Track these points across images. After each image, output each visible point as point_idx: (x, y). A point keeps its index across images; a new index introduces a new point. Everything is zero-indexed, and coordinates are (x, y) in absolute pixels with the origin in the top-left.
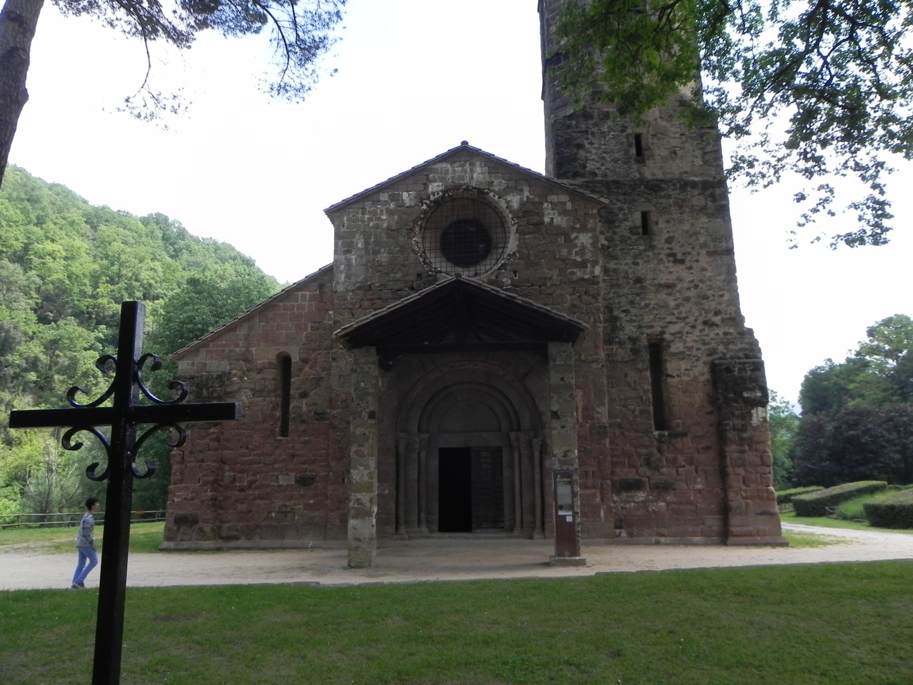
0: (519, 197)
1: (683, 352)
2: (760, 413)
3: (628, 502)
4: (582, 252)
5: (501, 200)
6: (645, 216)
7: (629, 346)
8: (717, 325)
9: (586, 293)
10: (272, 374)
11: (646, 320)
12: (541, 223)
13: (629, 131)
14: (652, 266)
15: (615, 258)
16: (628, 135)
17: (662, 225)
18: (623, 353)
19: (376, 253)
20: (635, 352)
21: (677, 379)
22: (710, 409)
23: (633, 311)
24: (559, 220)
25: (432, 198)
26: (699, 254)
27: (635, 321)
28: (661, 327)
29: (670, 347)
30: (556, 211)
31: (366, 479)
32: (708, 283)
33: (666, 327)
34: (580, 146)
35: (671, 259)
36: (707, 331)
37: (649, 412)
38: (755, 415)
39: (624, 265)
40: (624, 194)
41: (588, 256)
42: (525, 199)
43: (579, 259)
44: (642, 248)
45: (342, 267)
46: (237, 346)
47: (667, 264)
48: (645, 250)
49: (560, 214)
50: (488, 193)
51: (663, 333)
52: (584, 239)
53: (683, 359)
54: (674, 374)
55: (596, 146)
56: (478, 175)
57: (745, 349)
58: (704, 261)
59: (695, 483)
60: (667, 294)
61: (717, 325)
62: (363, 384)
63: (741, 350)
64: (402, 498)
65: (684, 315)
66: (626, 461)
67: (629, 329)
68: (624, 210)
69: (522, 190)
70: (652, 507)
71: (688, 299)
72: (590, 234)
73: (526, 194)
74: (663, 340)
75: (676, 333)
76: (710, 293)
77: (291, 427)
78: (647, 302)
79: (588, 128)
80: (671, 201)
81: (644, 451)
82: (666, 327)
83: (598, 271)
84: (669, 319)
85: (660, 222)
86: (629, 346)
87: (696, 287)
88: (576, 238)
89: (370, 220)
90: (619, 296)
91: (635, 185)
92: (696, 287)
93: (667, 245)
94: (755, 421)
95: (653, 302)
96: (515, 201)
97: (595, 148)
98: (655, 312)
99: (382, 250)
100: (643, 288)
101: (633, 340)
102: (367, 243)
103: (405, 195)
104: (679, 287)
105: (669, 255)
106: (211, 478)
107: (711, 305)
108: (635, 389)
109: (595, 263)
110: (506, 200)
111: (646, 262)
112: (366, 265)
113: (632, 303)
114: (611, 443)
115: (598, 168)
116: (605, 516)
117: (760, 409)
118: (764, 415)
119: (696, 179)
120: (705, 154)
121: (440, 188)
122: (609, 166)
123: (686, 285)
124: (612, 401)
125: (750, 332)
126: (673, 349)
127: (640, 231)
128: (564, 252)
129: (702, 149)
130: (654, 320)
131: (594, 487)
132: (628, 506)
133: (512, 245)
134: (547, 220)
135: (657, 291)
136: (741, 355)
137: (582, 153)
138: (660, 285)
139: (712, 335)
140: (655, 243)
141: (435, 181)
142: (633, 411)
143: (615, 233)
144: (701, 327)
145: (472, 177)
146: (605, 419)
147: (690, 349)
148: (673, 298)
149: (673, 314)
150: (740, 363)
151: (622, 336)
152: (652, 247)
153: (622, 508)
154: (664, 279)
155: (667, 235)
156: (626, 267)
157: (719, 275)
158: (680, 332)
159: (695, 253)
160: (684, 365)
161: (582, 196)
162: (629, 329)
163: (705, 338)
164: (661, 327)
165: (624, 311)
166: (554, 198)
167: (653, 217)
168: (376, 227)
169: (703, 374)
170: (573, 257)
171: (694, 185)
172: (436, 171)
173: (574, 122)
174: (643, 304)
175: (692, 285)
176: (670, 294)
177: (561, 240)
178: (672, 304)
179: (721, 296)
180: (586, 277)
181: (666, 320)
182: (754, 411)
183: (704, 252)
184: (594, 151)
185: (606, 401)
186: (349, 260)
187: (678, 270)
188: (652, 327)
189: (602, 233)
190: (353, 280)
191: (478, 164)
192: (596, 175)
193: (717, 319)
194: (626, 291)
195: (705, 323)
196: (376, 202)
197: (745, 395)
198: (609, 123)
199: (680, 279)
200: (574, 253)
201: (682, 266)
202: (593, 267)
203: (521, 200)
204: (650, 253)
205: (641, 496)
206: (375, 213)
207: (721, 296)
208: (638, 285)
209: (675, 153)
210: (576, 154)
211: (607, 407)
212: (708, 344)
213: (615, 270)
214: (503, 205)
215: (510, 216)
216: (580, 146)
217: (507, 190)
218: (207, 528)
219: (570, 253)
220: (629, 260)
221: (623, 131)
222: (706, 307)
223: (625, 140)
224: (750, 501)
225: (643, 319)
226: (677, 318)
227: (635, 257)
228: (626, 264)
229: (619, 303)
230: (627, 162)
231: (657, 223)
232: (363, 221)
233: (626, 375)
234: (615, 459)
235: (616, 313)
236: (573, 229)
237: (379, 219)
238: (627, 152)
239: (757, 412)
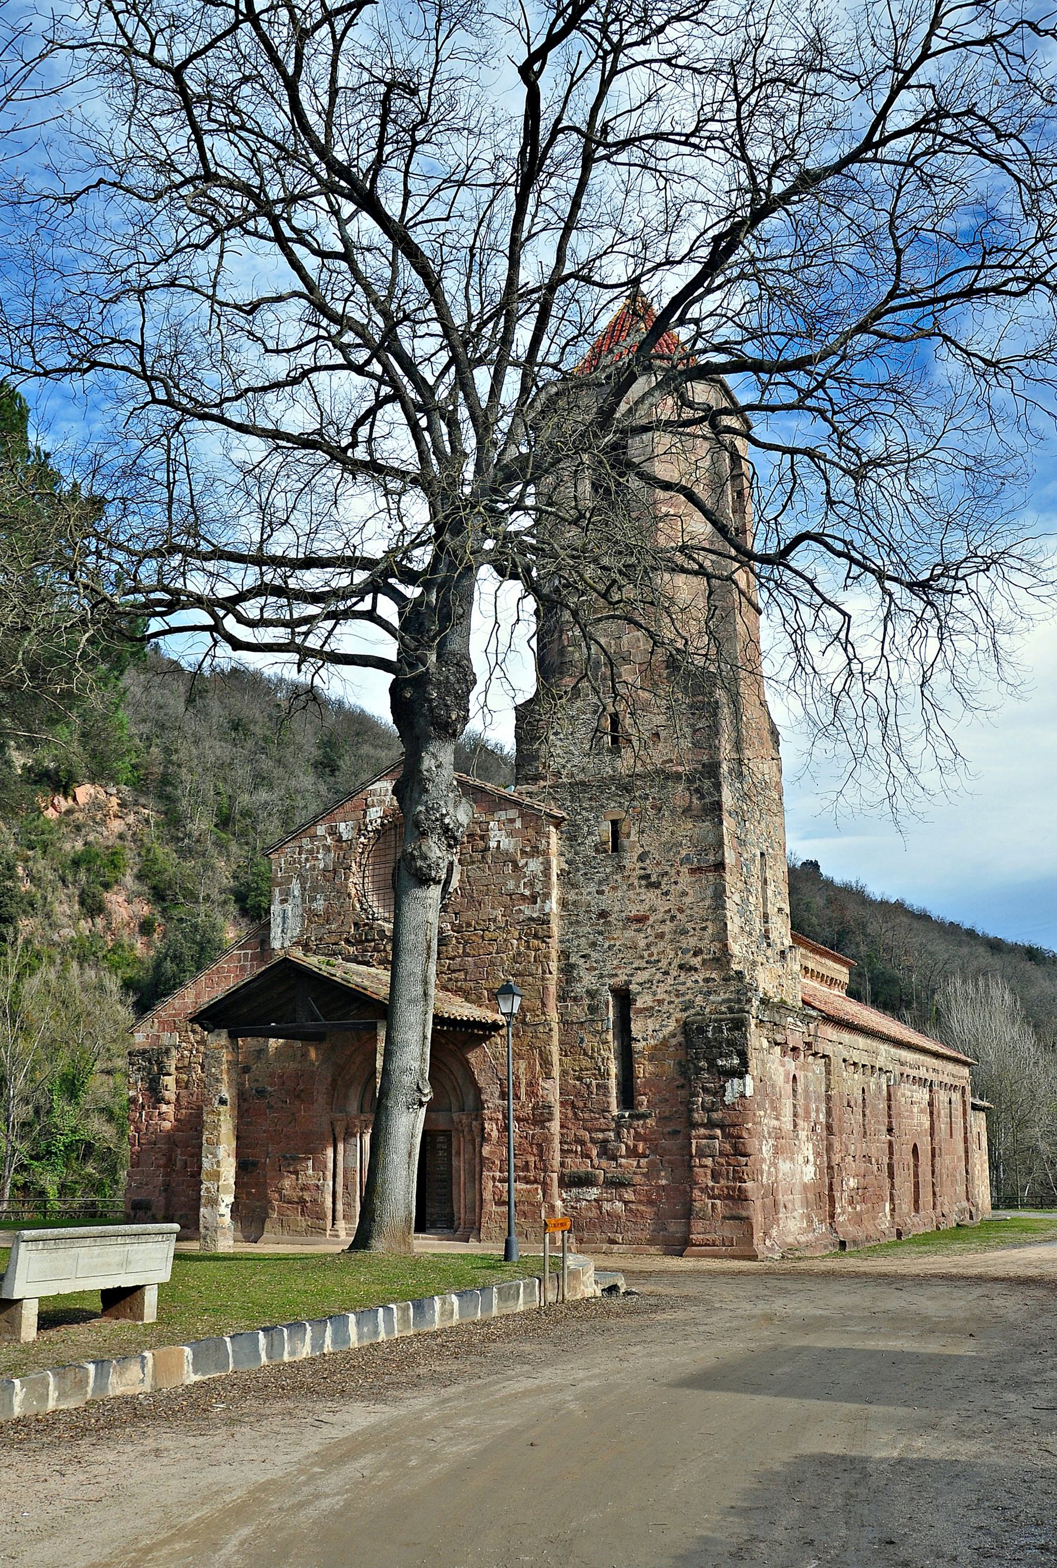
1: (652, 1008)
4: (531, 884)
6: (615, 823)
7: (587, 1001)
8: (696, 970)
9: (536, 936)
11: (609, 967)
12: (487, 849)
14: (620, 894)
15: (574, 886)
17: (634, 838)
18: (579, 1012)
19: (313, 899)
20: (593, 1009)
22: (681, 1081)
23: (595, 955)
24: (507, 844)
26: (678, 873)
32: (689, 912)
33: (632, 975)
35: (643, 882)
36: (682, 979)
37: (606, 1087)
38: (729, 1089)
39: (587, 893)
40: (590, 799)
43: (527, 893)
47: (638, 890)
51: (628, 983)
52: (534, 865)
57: (729, 1000)
58: (685, 879)
59: (659, 1178)
61: (696, 970)
63: (724, 1001)
65: (655, 957)
70: (607, 1206)
71: (661, 936)
74: (628, 991)
76: (689, 926)
81: (600, 1136)
82: (632, 975)
83: (553, 906)
85: (633, 832)
86: (587, 1001)
87: (673, 918)
89: (307, 860)
91: (603, 784)
92: (673, 918)
98: (621, 955)
100: (607, 923)
101: (592, 994)
102: (303, 889)
103: (343, 825)
104: (650, 922)
105: (641, 878)
106: (161, 1162)
107: (692, 942)
108: (592, 1058)
109: (547, 896)
111: (614, 888)
113: (593, 945)
114: (562, 1127)
117: (736, 1080)
118: (741, 1089)
119: (680, 769)
120: (695, 731)
122: (576, 762)
123: (660, 917)
124: (564, 1073)
126: (639, 1004)
128: (511, 885)
129: (692, 726)
130: (618, 967)
131: (536, 1182)
134: (493, 844)
135: (624, 928)
136: (724, 1009)
138: (628, 919)
139: (689, 984)
140: (625, 862)
141: (373, 806)
142: (589, 1086)
144: (676, 974)
147: (660, 1002)
149: (642, 957)
150: (716, 1021)
151: (579, 989)
154: (634, 910)
155: (641, 850)
157: (703, 900)
159: (674, 871)
160: (651, 1024)
162: (587, 980)
163: (680, 987)
165: (583, 956)
166: (502, 815)
167: (624, 828)
168: (313, 868)
169: (674, 1036)
170: (522, 890)
171: (678, 777)
174: (606, 945)
175: (667, 917)
176: (639, 931)
178: (642, 944)
179: (704, 929)
180: (535, 915)
183: (684, 870)
184: (559, 743)
185: (556, 1072)
187: (651, 897)
188: (616, 975)
189: (562, 854)
193: (696, 962)
194: (587, 929)
195: (681, 967)
196: (312, 838)
197: (720, 1063)
199: (653, 910)
201: (659, 891)
202: (544, 902)
204: (618, 877)
205: (594, 1193)
206: (310, 852)
207: (704, 929)
209: (657, 735)
210: (538, 750)
211: (558, 1082)
212: (683, 995)
213: (574, 903)
220: (593, 888)
222: (684, 946)
224: (718, 1202)
227: (600, 883)
231: (628, 835)
232: (300, 863)
234: (566, 1147)
235: (572, 960)
237: (317, 859)
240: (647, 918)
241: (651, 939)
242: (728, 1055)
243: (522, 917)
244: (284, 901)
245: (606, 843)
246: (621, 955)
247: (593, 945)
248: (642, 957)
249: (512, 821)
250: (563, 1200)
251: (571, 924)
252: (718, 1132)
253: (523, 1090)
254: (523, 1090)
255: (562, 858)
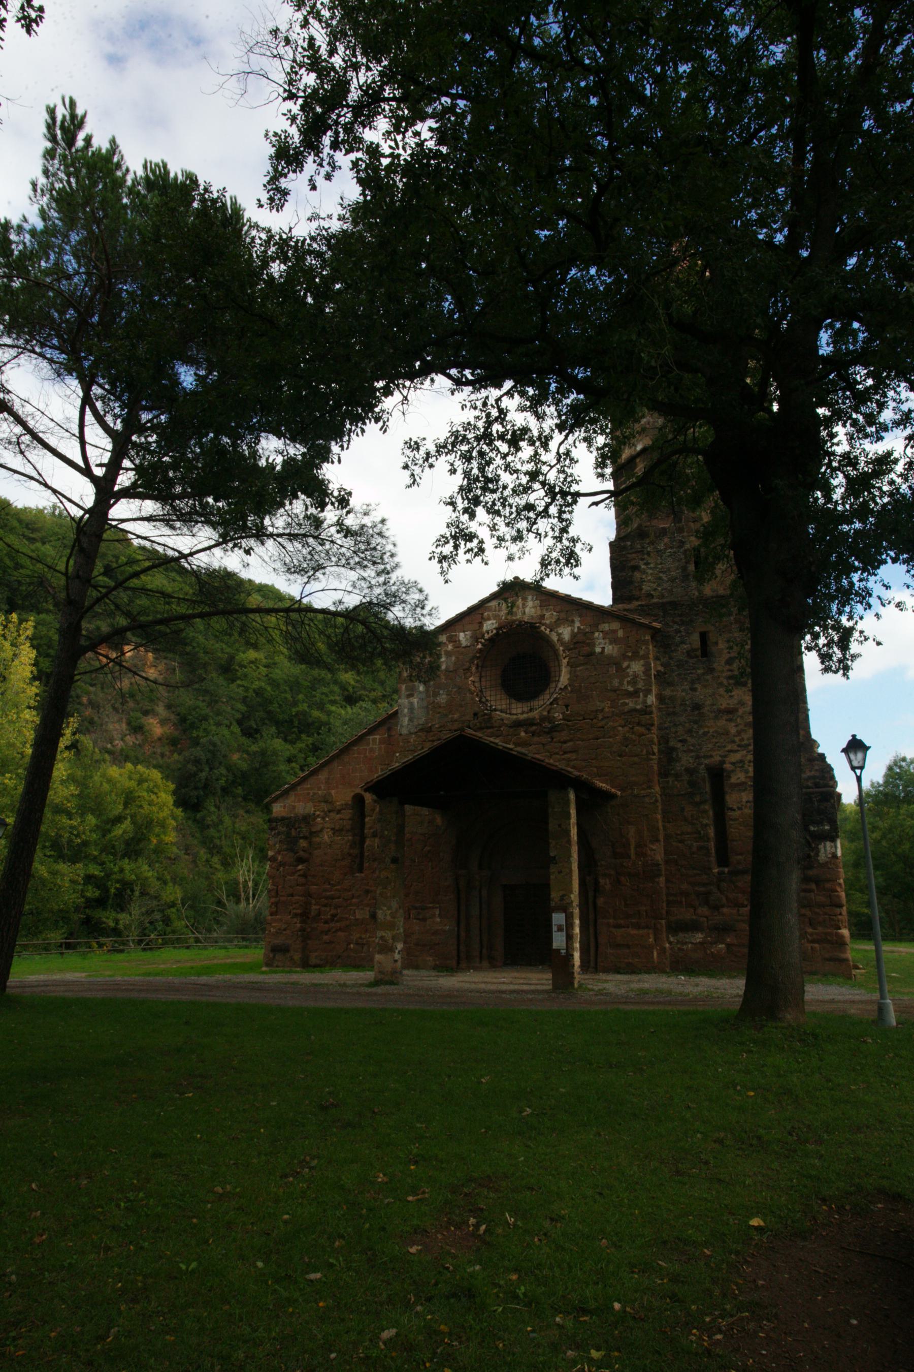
0: (569, 628)
2: (828, 848)
3: (686, 943)
4: (633, 682)
5: (553, 633)
6: (704, 636)
7: (686, 777)
9: (639, 724)
10: (347, 814)
12: (592, 654)
13: (687, 546)
15: (670, 684)
16: (686, 551)
17: (722, 645)
19: (436, 694)
21: (737, 813)
24: (610, 649)
25: (486, 636)
27: (692, 751)
28: (721, 756)
29: (730, 777)
30: (607, 641)
31: (388, 918)
33: (726, 756)
34: (636, 568)
38: (822, 850)
41: (640, 685)
42: (576, 630)
43: (631, 689)
44: (700, 672)
45: (406, 710)
46: (319, 789)
48: (704, 674)
49: (611, 643)
50: (539, 627)
52: (636, 667)
53: (744, 790)
54: (735, 807)
55: (652, 565)
56: (529, 609)
57: (814, 777)
60: (727, 720)
62: (386, 833)
64: (463, 934)
66: (684, 899)
67: (686, 760)
68: (680, 631)
69: (573, 621)
72: (642, 662)
73: (577, 624)
74: (722, 770)
75: (737, 762)
77: (366, 865)
78: (706, 730)
79: (643, 547)
80: (732, 618)
83: (652, 699)
84: (729, 747)
85: (720, 642)
86: (686, 777)
88: (628, 667)
90: (675, 725)
93: (727, 667)
94: (822, 857)
95: (711, 730)
96: (566, 632)
97: (651, 568)
98: (714, 740)
99: (441, 692)
101: (690, 771)
103: (462, 635)
104: (740, 712)
105: (729, 678)
109: (648, 692)
110: (557, 632)
111: (705, 686)
112: (427, 708)
113: (690, 731)
114: (667, 881)
115: (655, 590)
116: (658, 957)
117: (828, 844)
118: (833, 850)
121: (494, 626)
122: (665, 585)
125: (822, 757)
126: (733, 780)
127: (699, 653)
128: (616, 682)
131: (647, 927)
132: (685, 947)
133: (564, 678)
134: (598, 650)
136: (810, 784)
137: (637, 575)
138: (720, 711)
140: (715, 665)
141: (489, 619)
143: (671, 658)
145: (524, 613)
146: (659, 857)
148: (733, 724)
149: (734, 742)
152: (711, 670)
153: (679, 949)
154: (724, 703)
156: (684, 694)
158: (741, 761)
161: (633, 622)
162: (686, 760)
164: (721, 756)
165: (681, 741)
166: (606, 627)
172: (489, 609)
173: (629, 543)
174: (701, 732)
176: (730, 720)
177: (613, 670)
178: (733, 731)
180: (638, 707)
181: (727, 749)
182: (821, 847)
184: (650, 571)
186: (412, 704)
188: (711, 756)
190: (416, 723)
191: (530, 598)
192: (652, 596)
197: (812, 828)
198: (666, 540)
200: (625, 683)
202: (646, 696)
203: (572, 631)
204: (708, 677)
205: (699, 937)
208: (696, 712)
211: (662, 843)
214: (554, 638)
215: (561, 648)
216: (636, 568)
217: (559, 622)
218: (297, 957)
219: (621, 684)
221: (680, 547)
223: (682, 557)
224: (816, 945)
225: (701, 749)
226: (739, 746)
227: (693, 682)
228: (683, 691)
229: (676, 732)
230: (685, 577)
231: (716, 643)
233: (683, 809)
234: (671, 898)
235: (672, 744)
236: (624, 657)
238: (684, 569)
239: (825, 847)
240: (736, 710)
241: (741, 727)
242: (820, 823)
243: (626, 709)
244: (410, 696)
245: (696, 650)
246: (714, 740)
247: (690, 731)
248: (734, 742)
249: (615, 632)
250: (670, 943)
251: (669, 715)
252: (813, 886)
253: (632, 851)
254: (632, 851)
255: (658, 662)
